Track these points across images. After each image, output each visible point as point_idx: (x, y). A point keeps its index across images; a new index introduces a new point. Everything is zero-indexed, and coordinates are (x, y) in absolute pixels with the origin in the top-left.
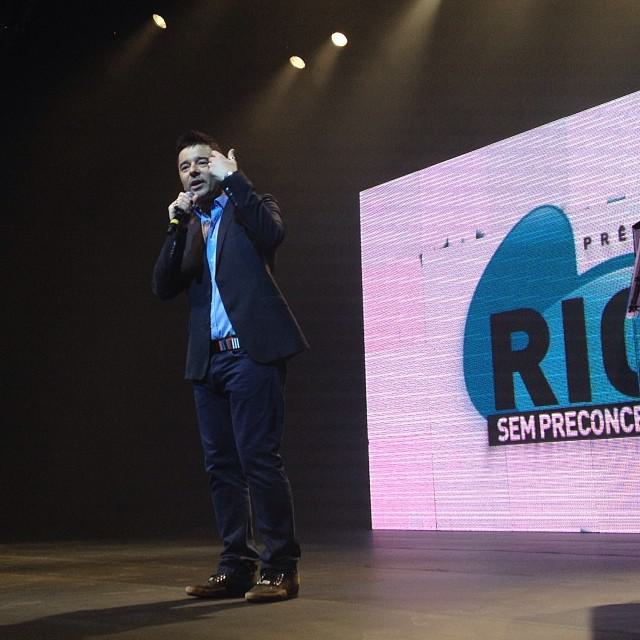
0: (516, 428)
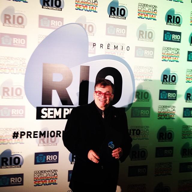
0: (52, 113)
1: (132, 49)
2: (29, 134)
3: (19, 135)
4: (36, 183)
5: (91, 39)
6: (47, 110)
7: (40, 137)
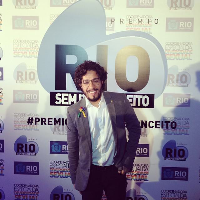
0: (66, 99)
1: (162, 23)
2: (44, 120)
3: (34, 121)
4: (52, 173)
5: (109, 14)
6: (62, 96)
7: (55, 124)
